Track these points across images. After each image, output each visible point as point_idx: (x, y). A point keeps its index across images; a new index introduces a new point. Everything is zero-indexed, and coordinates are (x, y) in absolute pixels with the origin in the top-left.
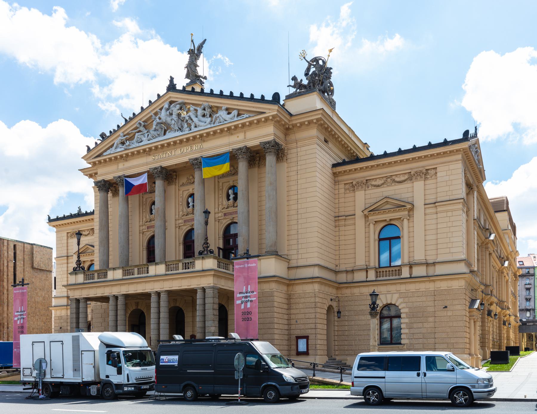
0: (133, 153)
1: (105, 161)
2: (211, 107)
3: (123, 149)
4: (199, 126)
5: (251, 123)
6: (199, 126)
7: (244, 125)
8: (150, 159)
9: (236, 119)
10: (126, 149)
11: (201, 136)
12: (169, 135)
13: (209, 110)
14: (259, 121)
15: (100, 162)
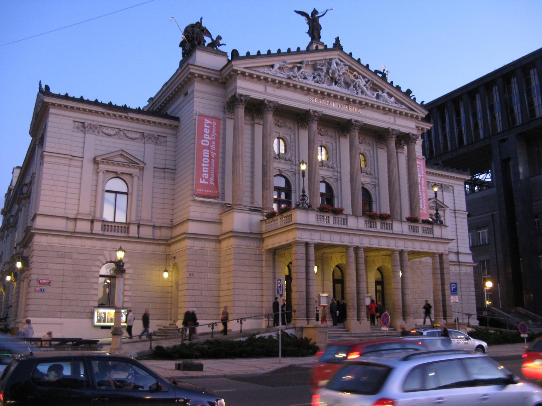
0: (295, 86)
1: (258, 77)
2: (374, 84)
3: (285, 76)
4: (366, 95)
5: (406, 114)
6: (366, 95)
7: (401, 113)
8: (306, 99)
9: (395, 105)
10: (289, 78)
11: (367, 104)
12: (334, 87)
13: (371, 85)
14: (412, 116)
15: (251, 75)
